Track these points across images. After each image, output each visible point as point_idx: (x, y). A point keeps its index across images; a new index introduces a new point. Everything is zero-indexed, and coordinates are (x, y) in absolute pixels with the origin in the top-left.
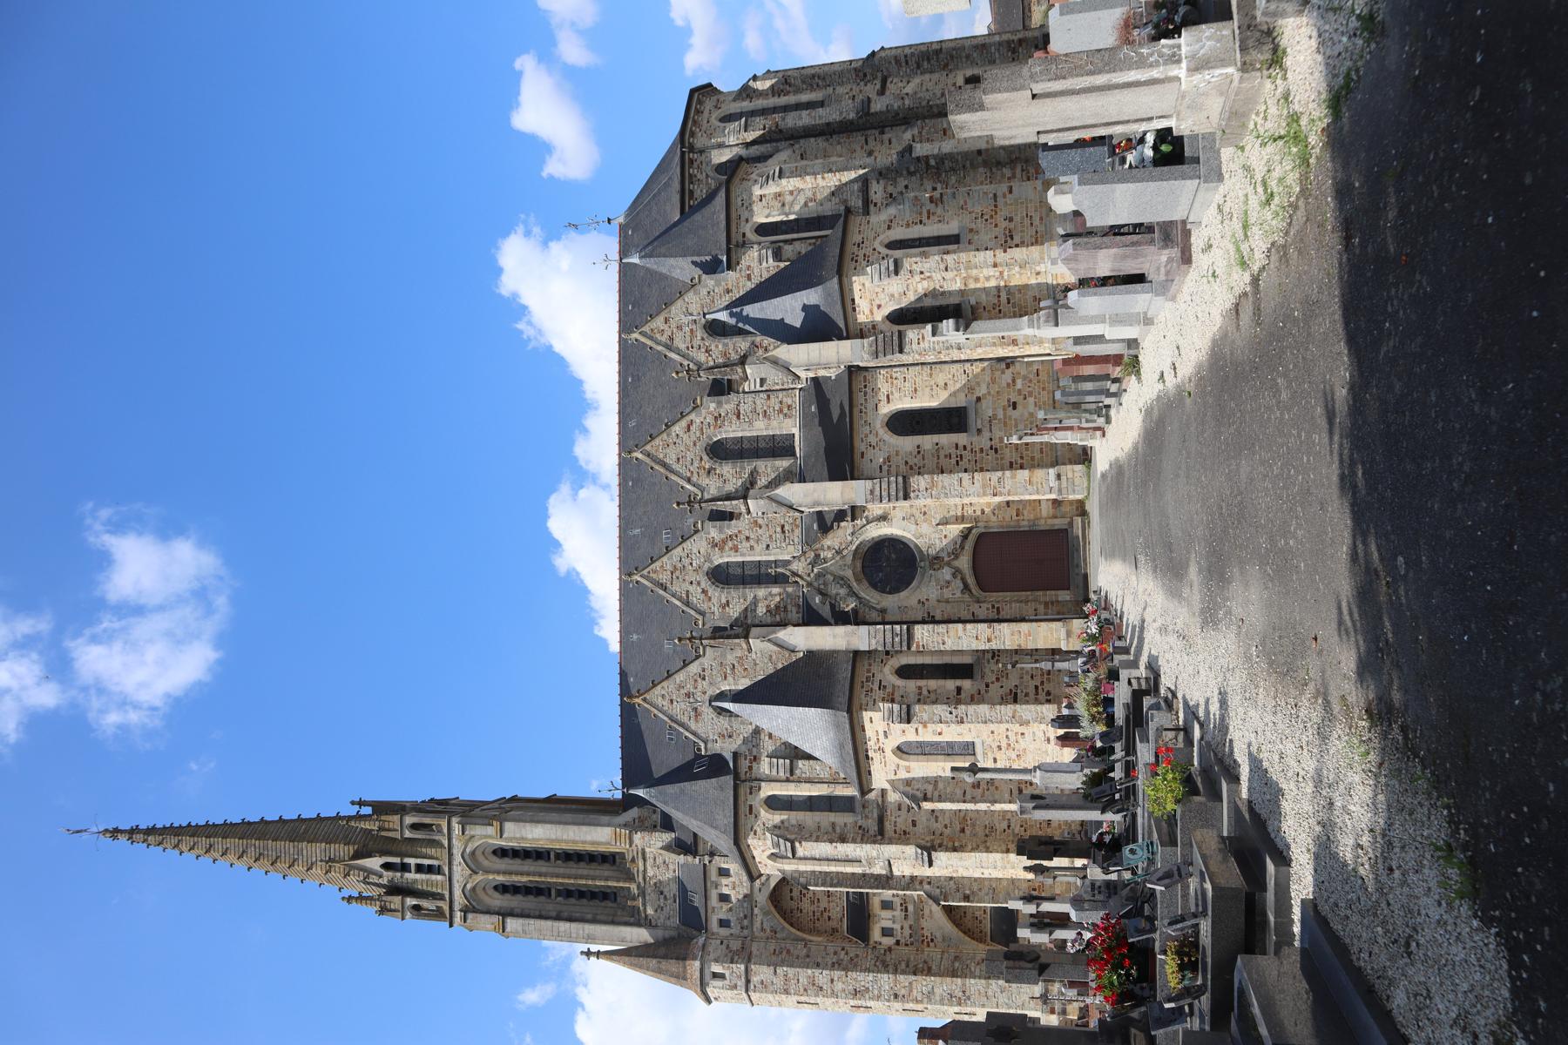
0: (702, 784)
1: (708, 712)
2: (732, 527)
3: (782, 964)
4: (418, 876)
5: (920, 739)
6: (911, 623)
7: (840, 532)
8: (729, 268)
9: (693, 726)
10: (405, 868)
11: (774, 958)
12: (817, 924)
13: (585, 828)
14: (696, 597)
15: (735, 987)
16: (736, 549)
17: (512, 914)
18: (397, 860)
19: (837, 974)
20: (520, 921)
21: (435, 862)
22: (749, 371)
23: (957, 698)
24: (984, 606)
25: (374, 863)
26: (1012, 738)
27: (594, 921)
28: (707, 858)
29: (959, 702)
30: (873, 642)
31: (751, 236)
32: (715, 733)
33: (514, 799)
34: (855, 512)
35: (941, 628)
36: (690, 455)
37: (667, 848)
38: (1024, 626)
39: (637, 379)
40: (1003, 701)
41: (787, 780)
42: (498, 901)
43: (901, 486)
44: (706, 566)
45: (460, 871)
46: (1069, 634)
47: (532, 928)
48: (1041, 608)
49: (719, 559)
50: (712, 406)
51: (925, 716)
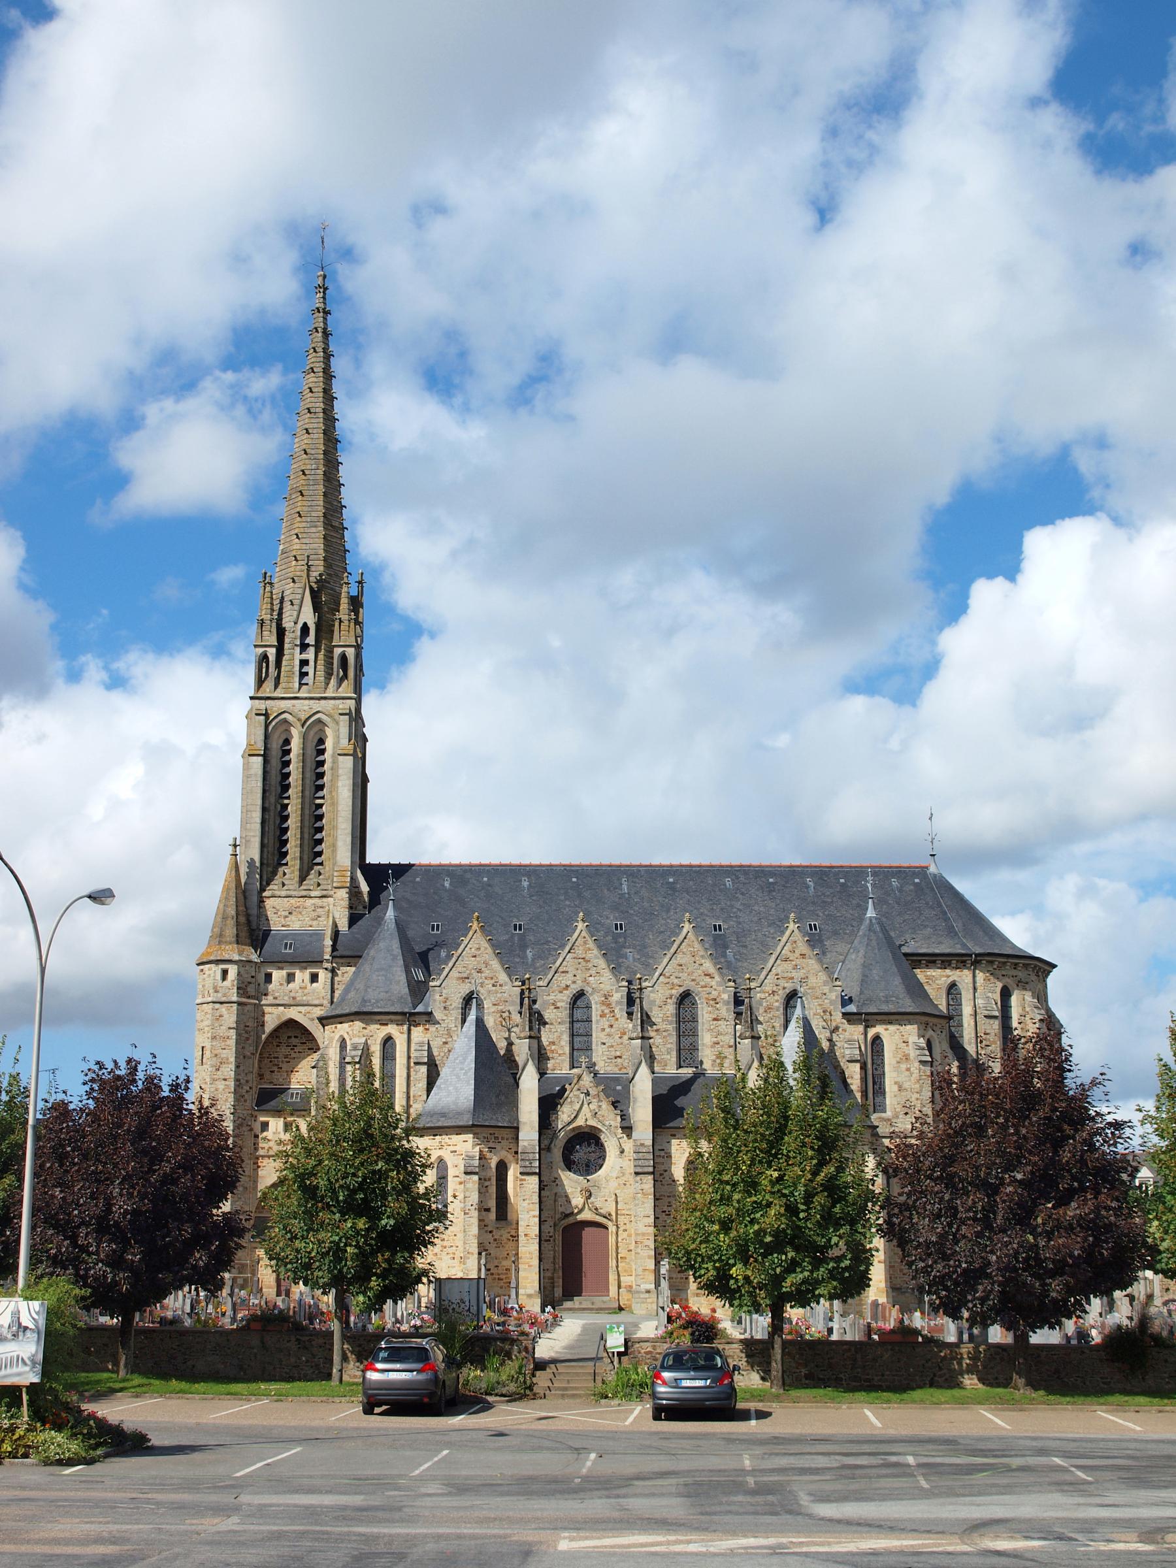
0: (403, 978)
1: (465, 989)
2: (621, 1012)
3: (238, 1034)
4: (297, 663)
5: (450, 1178)
6: (539, 1174)
7: (612, 1116)
8: (844, 1014)
9: (454, 974)
10: (304, 647)
11: (242, 1026)
12: (266, 1061)
13: (349, 839)
14: (562, 980)
15: (216, 991)
16: (603, 1015)
17: (266, 762)
18: (311, 640)
19: (232, 1084)
20: (260, 772)
21: (309, 679)
22: (746, 1041)
23: (483, 1209)
24: (552, 1230)
25: (308, 616)
26: (450, 1250)
27: (263, 846)
28: (328, 965)
29: (479, 1210)
30: (526, 1144)
31: (872, 1032)
32: (446, 991)
33: (365, 740)
34: (628, 1129)
35: (536, 1199)
36: (684, 976)
37: (335, 925)
38: (536, 1262)
39: (771, 888)
40: (480, 1244)
41: (409, 1058)
42: (276, 745)
43: (646, 1170)
44: (590, 990)
45: (303, 708)
46: (530, 1296)
47: (253, 784)
48: (549, 1274)
49: (595, 1000)
50: (725, 996)
51: (469, 1185)
